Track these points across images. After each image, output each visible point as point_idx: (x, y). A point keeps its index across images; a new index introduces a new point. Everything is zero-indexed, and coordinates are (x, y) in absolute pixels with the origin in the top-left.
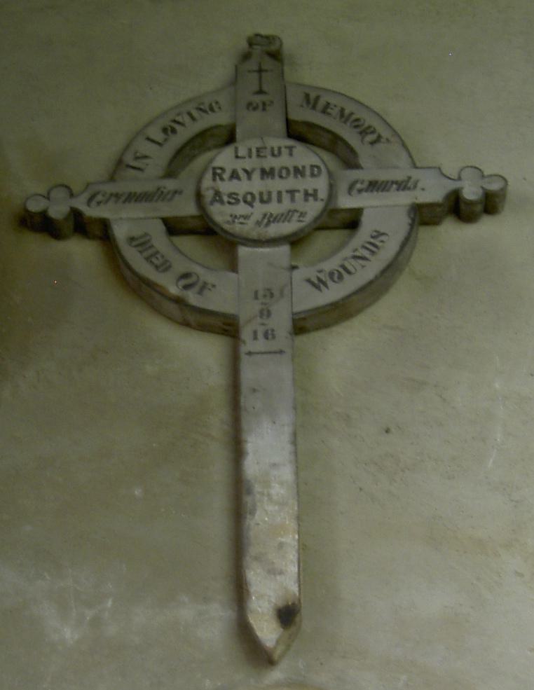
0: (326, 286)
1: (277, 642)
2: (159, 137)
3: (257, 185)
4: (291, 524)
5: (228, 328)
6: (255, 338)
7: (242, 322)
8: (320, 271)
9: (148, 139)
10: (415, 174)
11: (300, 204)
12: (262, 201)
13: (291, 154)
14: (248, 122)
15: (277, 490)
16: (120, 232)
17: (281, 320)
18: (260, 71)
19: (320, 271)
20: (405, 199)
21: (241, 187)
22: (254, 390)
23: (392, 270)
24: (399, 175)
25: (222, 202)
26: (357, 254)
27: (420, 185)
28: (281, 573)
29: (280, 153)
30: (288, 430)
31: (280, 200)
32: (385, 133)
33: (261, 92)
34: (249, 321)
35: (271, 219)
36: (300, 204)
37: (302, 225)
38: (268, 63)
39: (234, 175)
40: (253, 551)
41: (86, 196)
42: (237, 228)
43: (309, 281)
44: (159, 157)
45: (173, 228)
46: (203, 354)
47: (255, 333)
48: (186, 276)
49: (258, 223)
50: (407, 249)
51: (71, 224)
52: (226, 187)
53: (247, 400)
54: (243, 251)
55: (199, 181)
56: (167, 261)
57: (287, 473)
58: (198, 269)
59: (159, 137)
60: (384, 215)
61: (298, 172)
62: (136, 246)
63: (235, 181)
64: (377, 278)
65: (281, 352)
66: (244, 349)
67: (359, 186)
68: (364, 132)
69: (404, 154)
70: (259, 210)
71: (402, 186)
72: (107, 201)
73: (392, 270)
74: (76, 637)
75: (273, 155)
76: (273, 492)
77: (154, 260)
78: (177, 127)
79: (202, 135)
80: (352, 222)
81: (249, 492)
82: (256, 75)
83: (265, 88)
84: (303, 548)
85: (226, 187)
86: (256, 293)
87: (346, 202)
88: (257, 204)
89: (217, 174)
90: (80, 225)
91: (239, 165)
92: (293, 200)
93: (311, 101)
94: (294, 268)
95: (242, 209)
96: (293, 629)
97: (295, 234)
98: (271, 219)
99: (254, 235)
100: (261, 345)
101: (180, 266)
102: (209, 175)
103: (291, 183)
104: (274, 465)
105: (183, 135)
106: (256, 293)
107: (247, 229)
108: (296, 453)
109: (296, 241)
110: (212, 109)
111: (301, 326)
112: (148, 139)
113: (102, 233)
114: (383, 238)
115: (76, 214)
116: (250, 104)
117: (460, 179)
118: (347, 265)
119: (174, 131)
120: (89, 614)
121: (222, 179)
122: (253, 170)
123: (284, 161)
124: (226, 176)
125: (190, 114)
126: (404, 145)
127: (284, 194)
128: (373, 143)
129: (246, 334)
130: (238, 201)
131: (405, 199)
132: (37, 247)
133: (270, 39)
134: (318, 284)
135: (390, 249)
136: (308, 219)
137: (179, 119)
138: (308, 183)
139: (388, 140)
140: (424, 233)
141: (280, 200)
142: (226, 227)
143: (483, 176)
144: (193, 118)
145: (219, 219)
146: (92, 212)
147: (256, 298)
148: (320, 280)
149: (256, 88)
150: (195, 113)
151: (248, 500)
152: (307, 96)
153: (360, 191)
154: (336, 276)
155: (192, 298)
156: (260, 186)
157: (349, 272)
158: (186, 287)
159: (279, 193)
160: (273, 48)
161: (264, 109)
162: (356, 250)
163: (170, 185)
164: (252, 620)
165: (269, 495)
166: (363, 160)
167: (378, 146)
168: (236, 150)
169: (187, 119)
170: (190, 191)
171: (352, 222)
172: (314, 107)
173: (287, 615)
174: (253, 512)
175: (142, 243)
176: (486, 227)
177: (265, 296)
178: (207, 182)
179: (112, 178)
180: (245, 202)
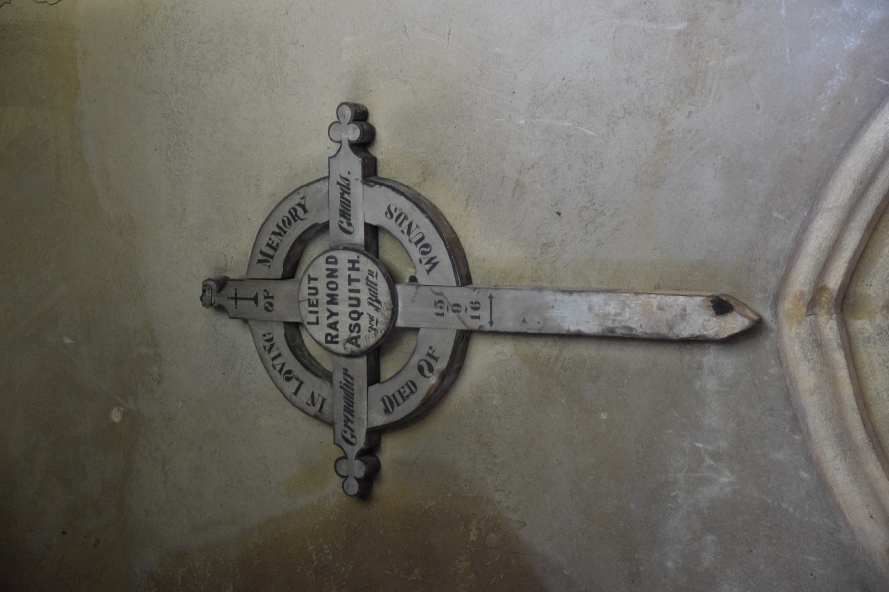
0: (432, 258)
1: (745, 316)
2: (294, 384)
3: (343, 308)
4: (643, 298)
5: (464, 338)
6: (478, 317)
7: (464, 328)
8: (421, 262)
9: (296, 393)
10: (335, 178)
11: (361, 275)
12: (358, 305)
13: (316, 279)
14: (283, 310)
15: (612, 308)
16: (380, 419)
17: (463, 295)
18: (236, 299)
19: (421, 262)
20: (357, 188)
21: (344, 322)
22: (524, 321)
23: (418, 202)
24: (336, 192)
25: (359, 337)
26: (406, 231)
27: (345, 175)
28: (684, 309)
29: (315, 288)
30: (560, 296)
31: (358, 291)
32: (297, 199)
33: (256, 299)
34: (463, 322)
35: (374, 299)
36: (361, 275)
37: (380, 273)
38: (230, 291)
39: (334, 326)
40: (664, 331)
41: (345, 446)
42: (382, 327)
43: (428, 271)
44: (312, 384)
45: (374, 378)
46: (483, 356)
47: (473, 317)
48: (421, 369)
49: (377, 309)
50: (402, 189)
51: (369, 458)
52: (344, 333)
53: (532, 327)
54: (400, 323)
55: (338, 354)
56: (407, 384)
57: (597, 300)
58: (415, 360)
59: (294, 384)
60: (371, 206)
61: (332, 274)
62: (393, 408)
63: (338, 326)
64: (428, 217)
65: (491, 297)
66: (488, 327)
67: (345, 225)
68: (296, 217)
69: (317, 185)
70: (365, 308)
71: (345, 189)
72: (352, 430)
73: (418, 202)
74: (728, 473)
75: (316, 294)
76: (613, 312)
77: (405, 395)
78: (286, 369)
79: (293, 349)
80: (373, 231)
81: (612, 330)
82: (239, 302)
83: (252, 296)
84: (657, 289)
85: (344, 333)
86: (437, 314)
87: (359, 236)
88: (359, 310)
89: (332, 339)
90: (370, 452)
91: (324, 321)
92: (357, 280)
93: (266, 259)
94: (413, 279)
95: (364, 322)
96: (732, 302)
97: (388, 281)
98: (374, 299)
99: (388, 314)
100: (484, 313)
101: (412, 373)
102: (332, 347)
103: (342, 282)
104: (590, 309)
105: (292, 363)
106: (437, 314)
107: (382, 318)
108: (580, 291)
109: (392, 279)
110: (271, 340)
111: (465, 278)
112: (296, 393)
113: (376, 435)
114: (392, 210)
115: (361, 455)
116: (267, 309)
117: (340, 142)
118: (415, 240)
119: (290, 372)
120: (709, 461)
121: (337, 336)
122: (329, 310)
123: (321, 285)
124: (334, 333)
125: (274, 359)
126: (308, 185)
127: (351, 287)
128: (305, 211)
129: (474, 324)
130: (357, 325)
131: (357, 188)
132: (387, 487)
133: (205, 288)
134: (432, 264)
135: (402, 203)
136: (375, 269)
137: (278, 367)
138: (343, 267)
139: (303, 198)
140: (384, 171)
141: (358, 291)
142: (380, 335)
143: (339, 122)
144: (279, 355)
145: (372, 341)
146: (361, 441)
147: (442, 315)
148: (428, 263)
149: (252, 303)
150: (274, 353)
151: (619, 332)
152: (260, 261)
153: (349, 225)
154: (425, 248)
155: (441, 365)
156: (341, 304)
157: (422, 239)
158: (431, 370)
159: (351, 291)
160: (214, 286)
161: (272, 297)
162: (403, 232)
163: (339, 377)
164: (724, 335)
165: (616, 315)
166: (321, 220)
167: (307, 207)
168: (312, 323)
169: (279, 361)
170: (344, 362)
171: (373, 231)
172: (271, 257)
173: (721, 307)
174: (631, 329)
175: (390, 403)
176: (376, 119)
177: (441, 308)
178: (339, 348)
179: (332, 424)
180: (357, 319)
